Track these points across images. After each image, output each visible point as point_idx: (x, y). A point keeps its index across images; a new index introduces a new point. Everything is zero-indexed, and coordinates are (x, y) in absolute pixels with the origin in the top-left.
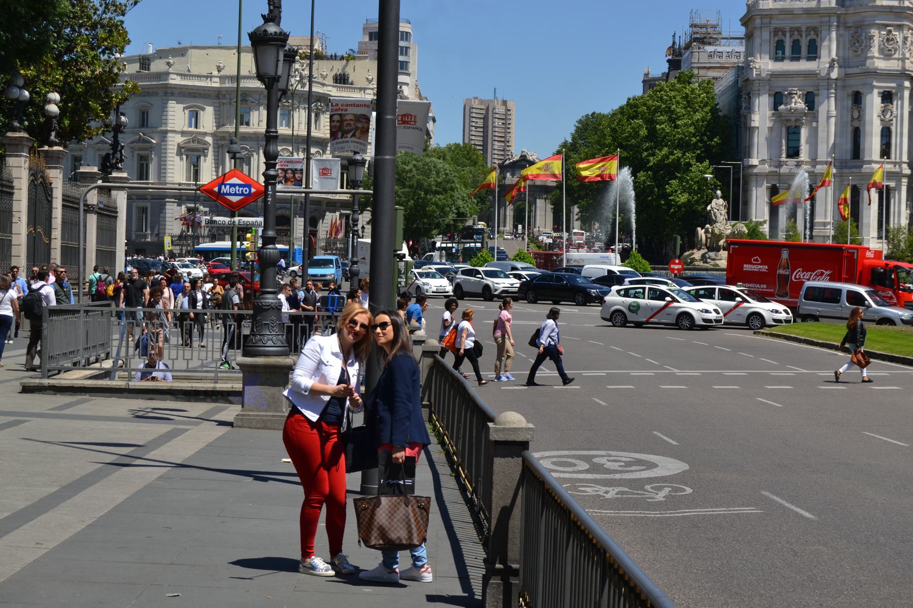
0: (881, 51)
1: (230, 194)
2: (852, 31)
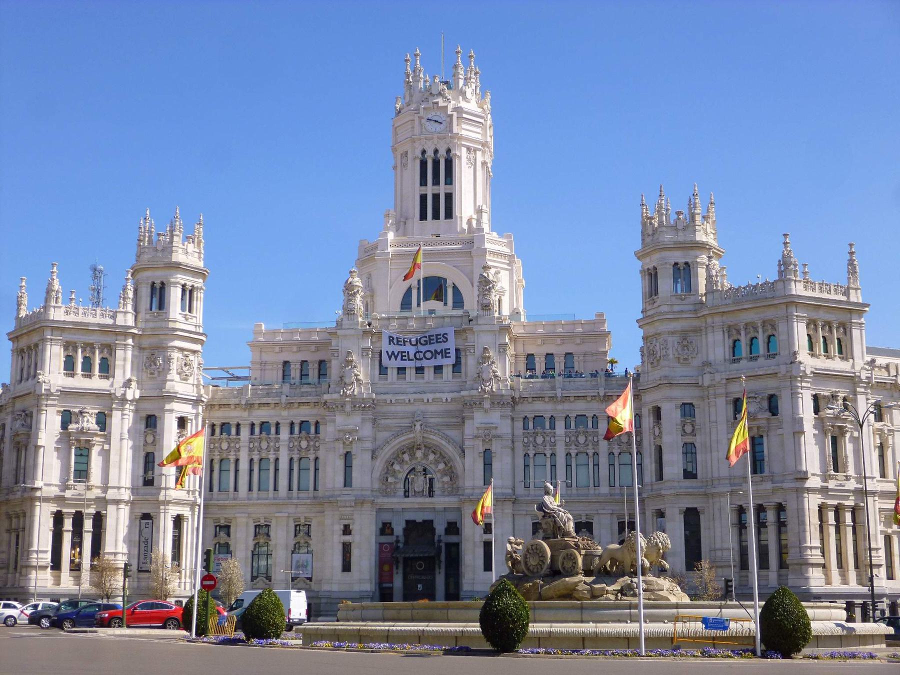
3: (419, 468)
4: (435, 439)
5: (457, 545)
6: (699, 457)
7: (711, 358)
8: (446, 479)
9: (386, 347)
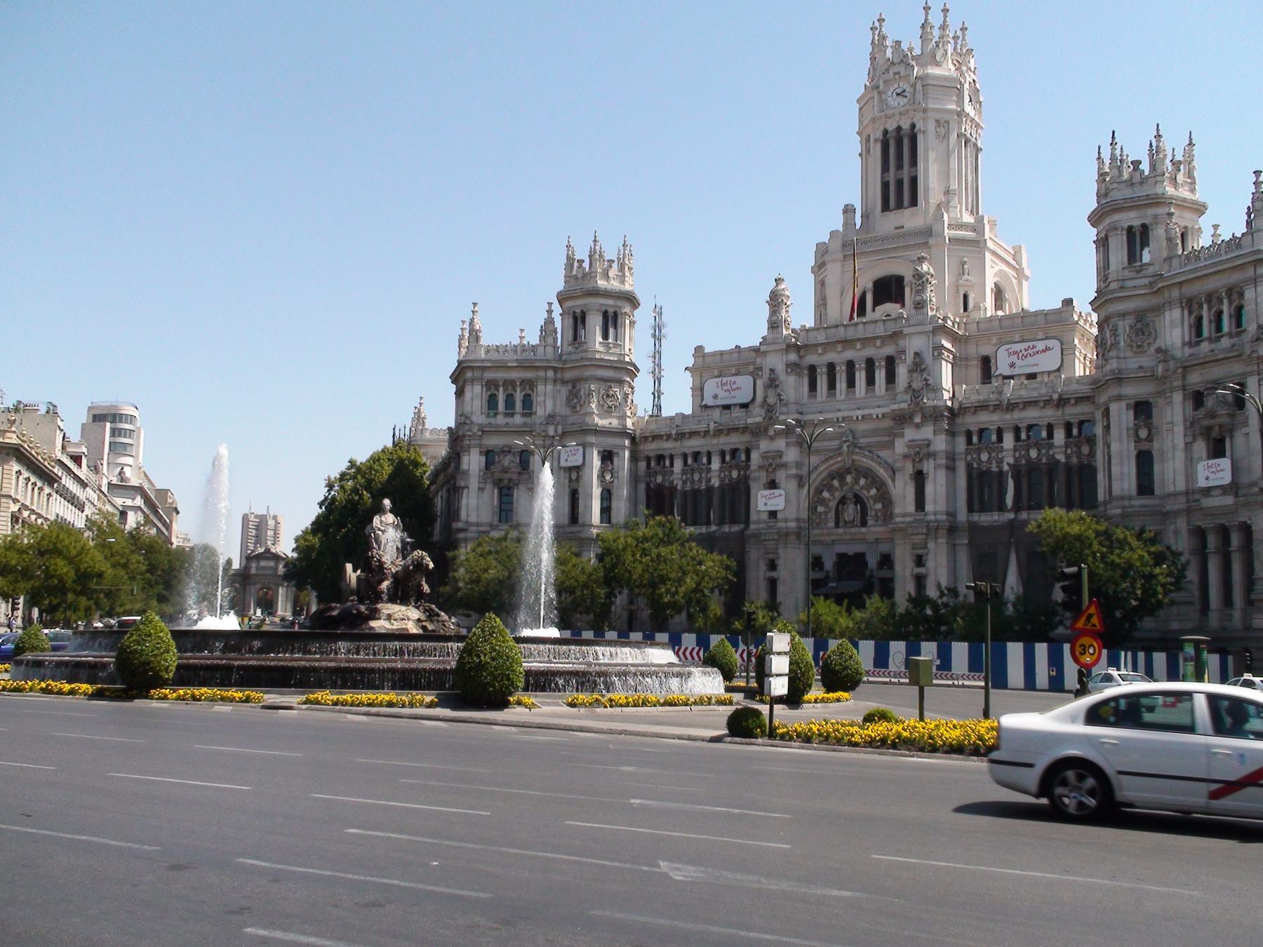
0: (600, 406)
2: (570, 387)
3: (850, 495)
4: (865, 461)
5: (891, 580)
6: (1156, 468)
7: (1169, 342)
8: (879, 506)
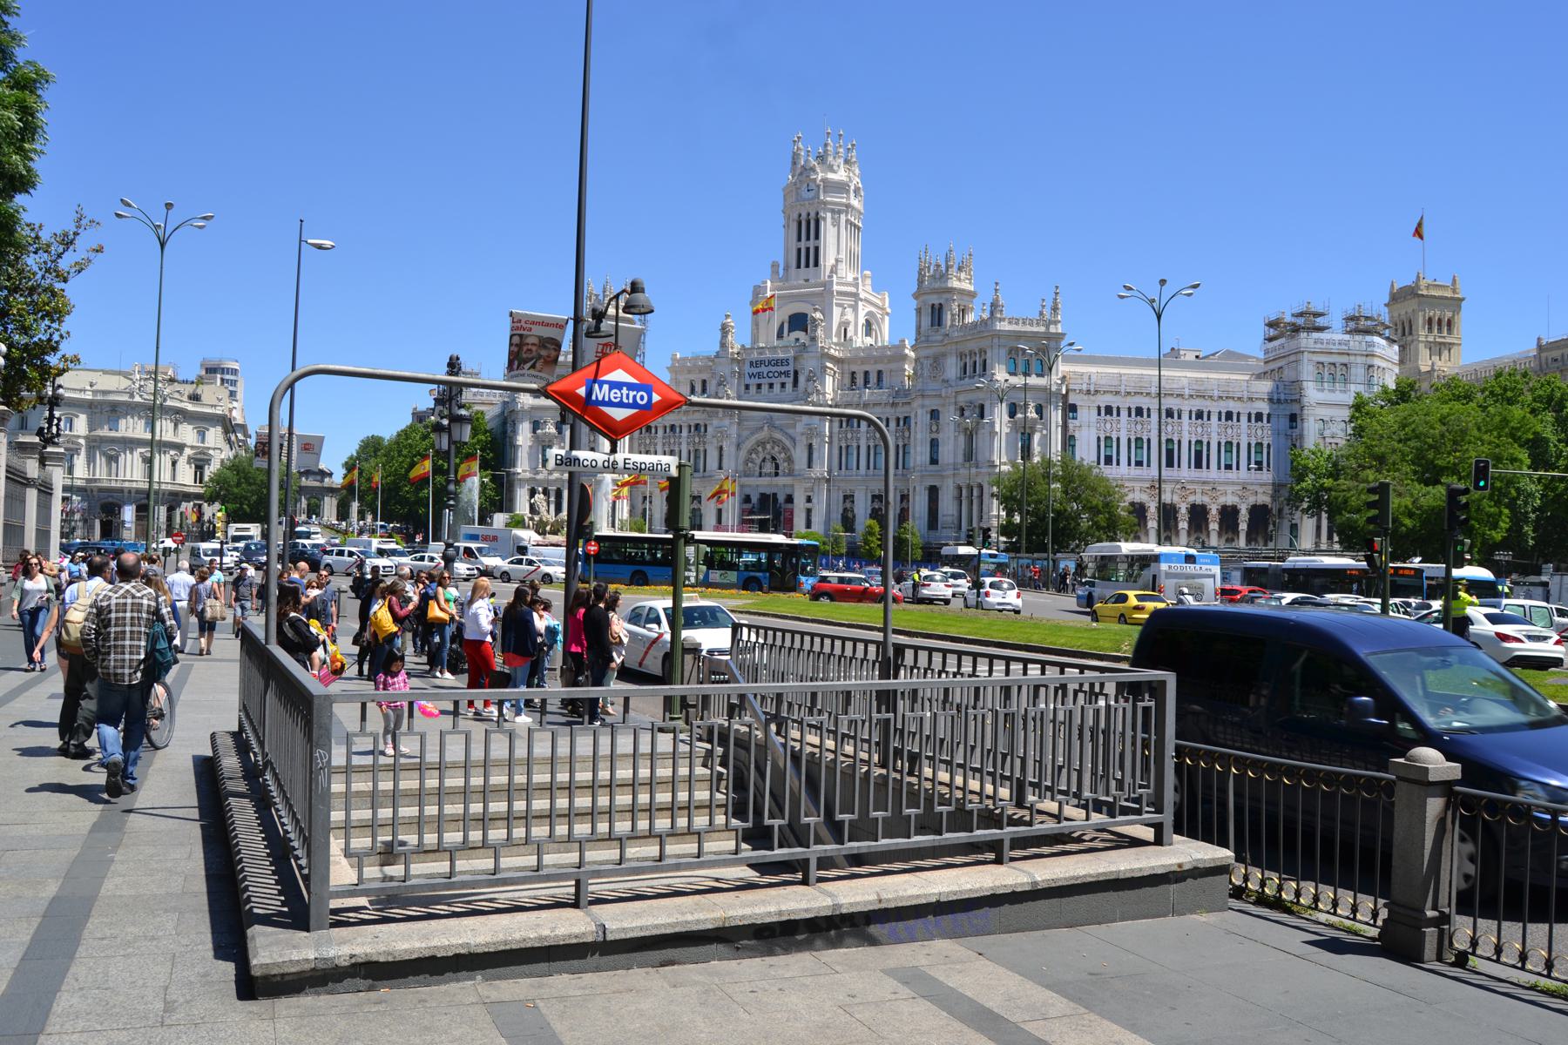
1: (610, 404)
4: (778, 435)
9: (747, 369)
